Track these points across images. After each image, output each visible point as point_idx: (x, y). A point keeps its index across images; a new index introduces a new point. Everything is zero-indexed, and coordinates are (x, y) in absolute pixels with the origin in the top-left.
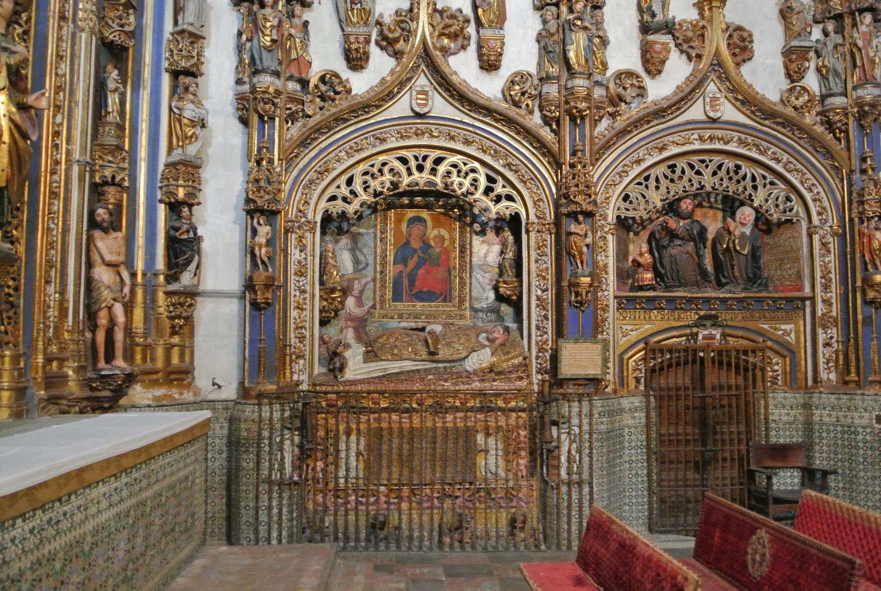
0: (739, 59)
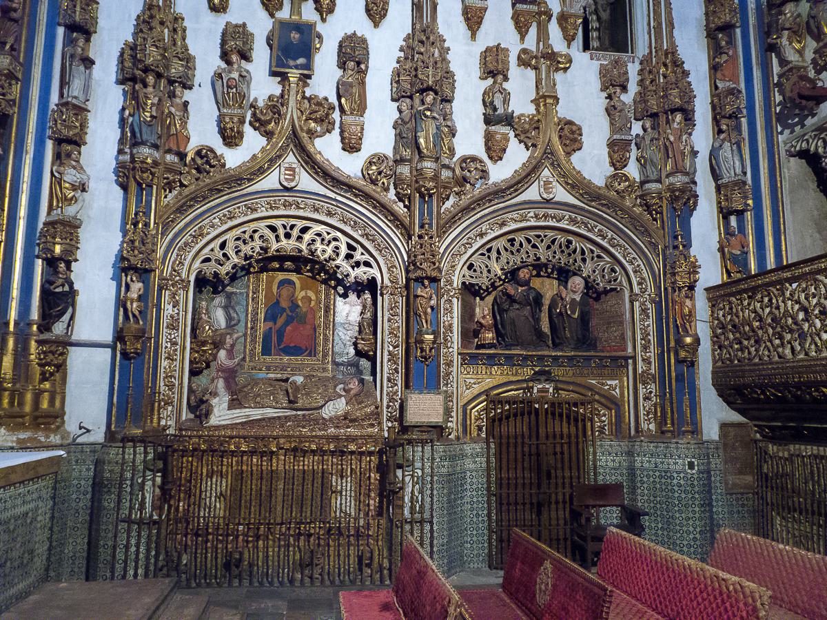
0: (569, 149)
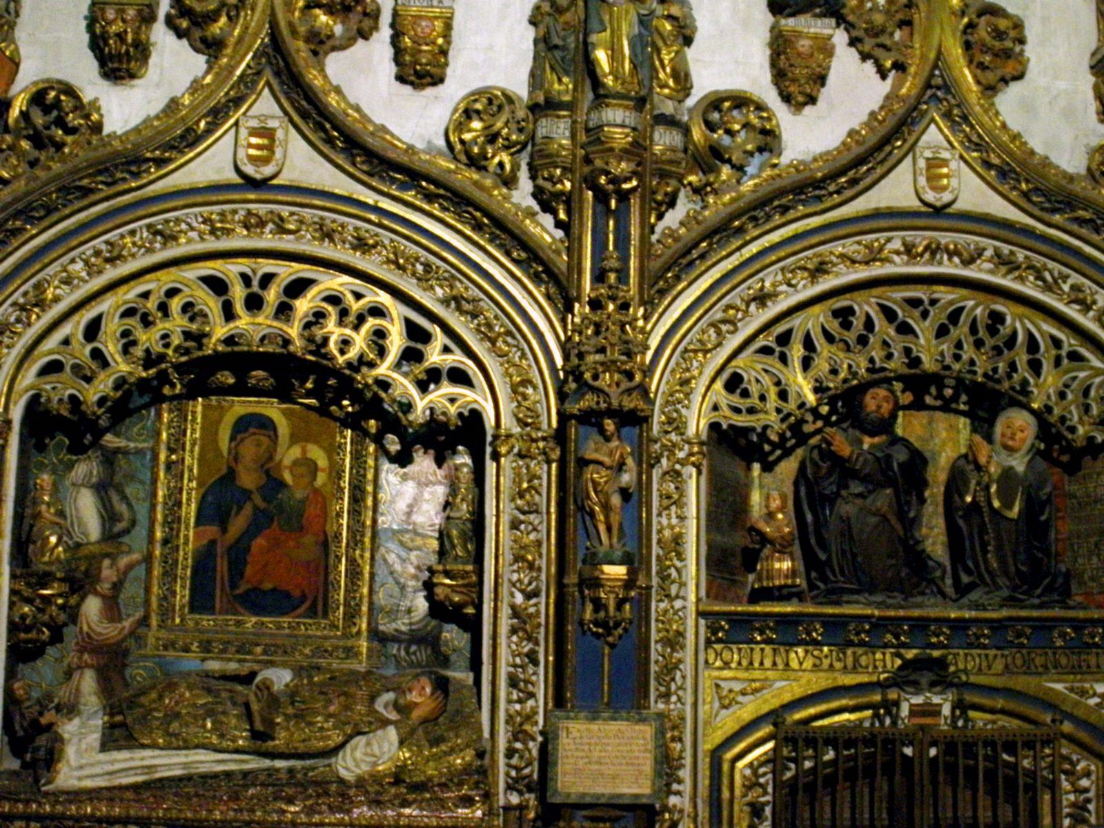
0: (990, 77)
